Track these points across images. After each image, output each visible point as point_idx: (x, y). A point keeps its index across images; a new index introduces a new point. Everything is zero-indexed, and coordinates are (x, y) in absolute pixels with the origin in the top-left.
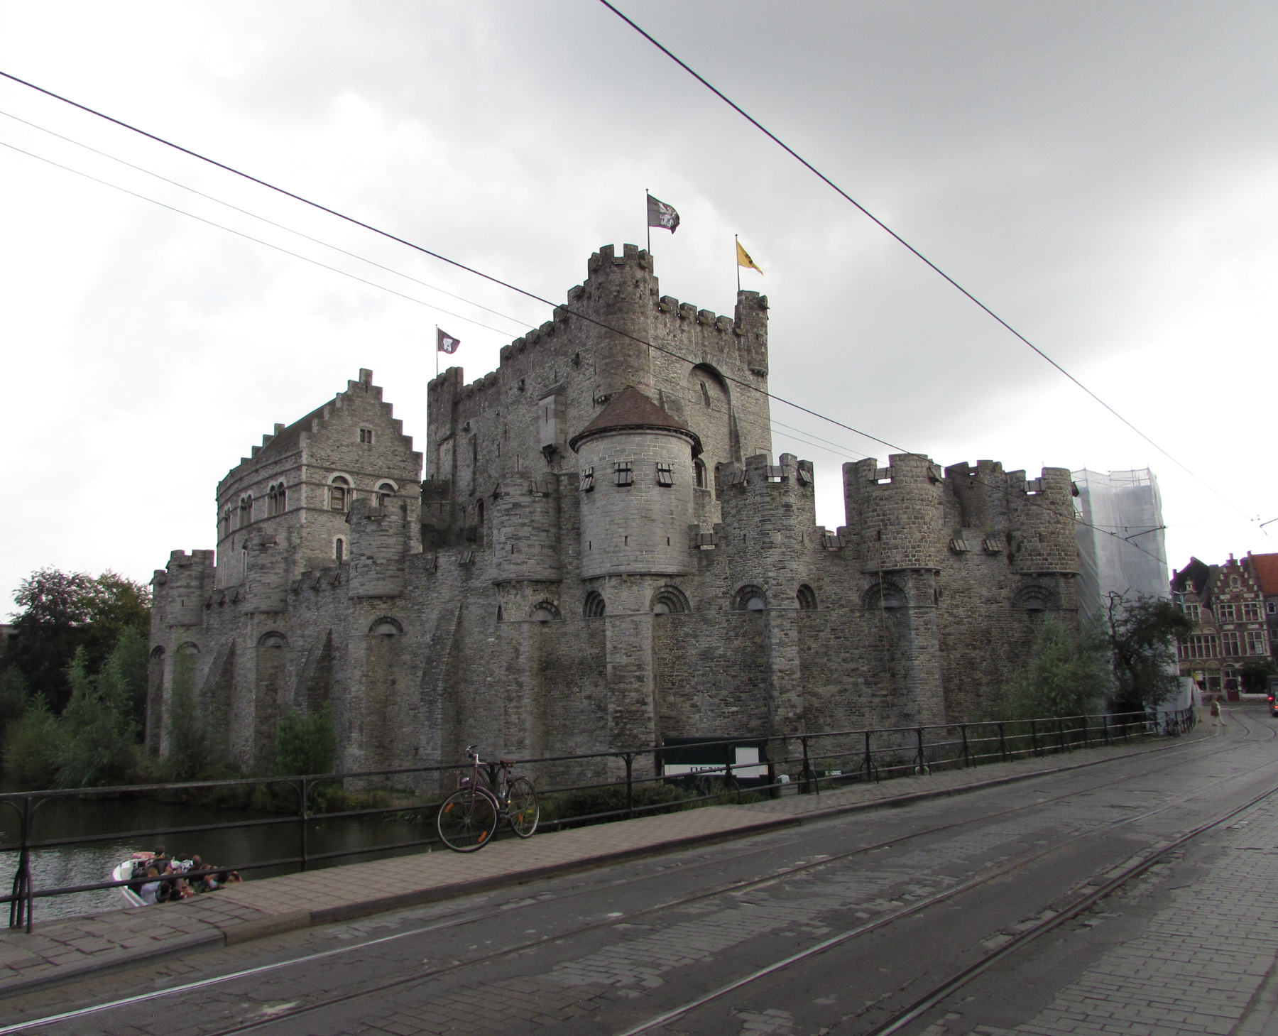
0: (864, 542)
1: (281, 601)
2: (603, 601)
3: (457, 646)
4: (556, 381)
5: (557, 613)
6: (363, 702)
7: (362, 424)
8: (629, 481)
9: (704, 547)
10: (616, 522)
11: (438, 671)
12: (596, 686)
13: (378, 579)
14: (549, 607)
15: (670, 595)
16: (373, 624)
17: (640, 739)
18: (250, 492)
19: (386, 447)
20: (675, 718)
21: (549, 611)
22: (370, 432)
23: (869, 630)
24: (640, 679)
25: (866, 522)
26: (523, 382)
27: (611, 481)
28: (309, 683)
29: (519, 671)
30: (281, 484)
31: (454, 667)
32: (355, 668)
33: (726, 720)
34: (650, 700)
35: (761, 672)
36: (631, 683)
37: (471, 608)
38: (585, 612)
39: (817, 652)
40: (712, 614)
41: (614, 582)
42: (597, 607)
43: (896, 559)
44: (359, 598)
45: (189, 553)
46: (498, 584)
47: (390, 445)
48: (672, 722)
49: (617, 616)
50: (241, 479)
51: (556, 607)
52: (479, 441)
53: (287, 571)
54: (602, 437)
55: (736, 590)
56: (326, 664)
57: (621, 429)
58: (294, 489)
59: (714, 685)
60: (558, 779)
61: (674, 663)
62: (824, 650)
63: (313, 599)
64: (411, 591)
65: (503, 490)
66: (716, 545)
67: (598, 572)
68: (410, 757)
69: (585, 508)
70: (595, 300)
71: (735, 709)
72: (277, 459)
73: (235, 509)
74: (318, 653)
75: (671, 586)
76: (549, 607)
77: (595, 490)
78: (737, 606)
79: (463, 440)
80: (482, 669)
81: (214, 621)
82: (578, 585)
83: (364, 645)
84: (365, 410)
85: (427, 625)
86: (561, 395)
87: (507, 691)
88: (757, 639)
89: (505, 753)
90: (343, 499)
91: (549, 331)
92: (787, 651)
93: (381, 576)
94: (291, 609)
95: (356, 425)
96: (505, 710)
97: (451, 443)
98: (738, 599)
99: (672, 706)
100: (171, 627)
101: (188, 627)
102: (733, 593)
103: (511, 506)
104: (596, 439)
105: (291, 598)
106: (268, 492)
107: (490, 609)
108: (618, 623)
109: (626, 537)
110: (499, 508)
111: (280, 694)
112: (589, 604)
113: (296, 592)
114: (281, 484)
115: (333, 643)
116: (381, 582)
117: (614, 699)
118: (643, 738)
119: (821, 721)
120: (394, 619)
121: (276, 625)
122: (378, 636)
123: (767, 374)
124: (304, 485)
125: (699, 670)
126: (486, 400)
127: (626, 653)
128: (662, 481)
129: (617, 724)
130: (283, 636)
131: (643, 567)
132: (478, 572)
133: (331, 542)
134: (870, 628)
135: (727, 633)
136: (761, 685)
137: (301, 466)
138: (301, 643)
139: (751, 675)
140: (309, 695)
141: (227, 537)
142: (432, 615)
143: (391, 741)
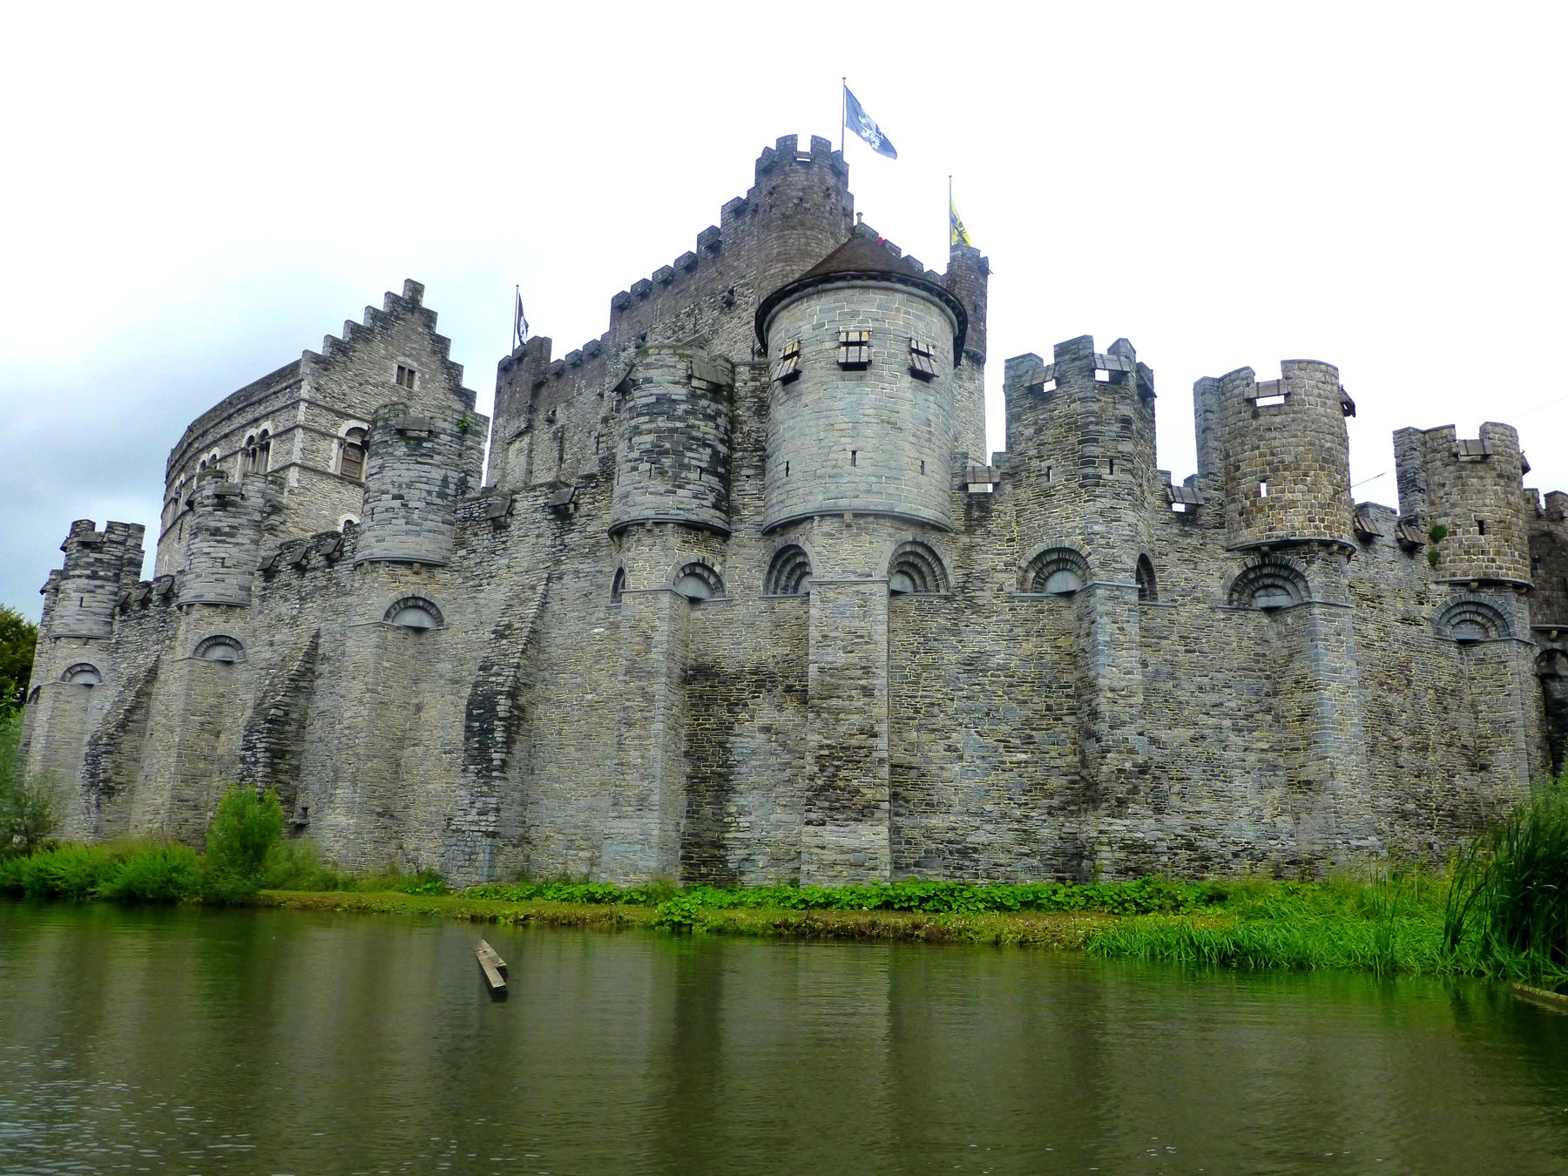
0: (1234, 501)
1: (241, 588)
2: (804, 564)
3: (534, 638)
4: (696, 332)
5: (718, 586)
6: (363, 734)
7: (401, 359)
8: (864, 359)
9: (973, 489)
10: (836, 427)
11: (501, 680)
12: (779, 711)
13: (407, 533)
14: (706, 574)
15: (918, 561)
16: (393, 606)
17: (864, 795)
18: (216, 451)
19: (435, 399)
20: (918, 769)
21: (706, 582)
22: (412, 373)
23: (1239, 647)
24: (867, 692)
25: (1238, 468)
26: (643, 338)
27: (832, 360)
28: (272, 711)
29: (651, 674)
30: (265, 432)
31: (529, 675)
32: (354, 678)
33: (1007, 774)
34: (882, 728)
35: (1068, 696)
36: (851, 698)
37: (566, 579)
38: (766, 586)
39: (1157, 672)
40: (985, 597)
41: (829, 525)
42: (787, 578)
43: (1294, 524)
44: (372, 562)
45: (101, 528)
46: (619, 532)
47: (442, 397)
48: (913, 773)
49: (831, 583)
50: (204, 434)
51: (716, 576)
52: (567, 435)
53: (256, 542)
54: (819, 292)
55: (1031, 559)
56: (302, 684)
57: (854, 278)
58: (284, 437)
59: (988, 714)
60: (704, 870)
61: (918, 676)
62: (1168, 668)
63: (295, 582)
64: (464, 558)
65: (640, 375)
66: (996, 485)
67: (799, 509)
68: (436, 834)
69: (779, 412)
70: (765, 211)
71: (1023, 757)
72: (261, 397)
73: (194, 476)
74: (296, 666)
75: (922, 544)
76: (706, 574)
77: (802, 378)
78: (1028, 585)
79: (543, 434)
80: (579, 680)
81: (132, 634)
82: (758, 540)
83: (374, 639)
84: (407, 338)
85: (486, 611)
86: (702, 348)
87: (625, 709)
88: (1062, 642)
89: (614, 818)
90: (361, 464)
91: (689, 264)
92: (1121, 656)
93: (418, 528)
94: (256, 601)
95: (392, 358)
96: (619, 743)
97: (526, 439)
98: (1032, 574)
99: (912, 747)
100: (57, 638)
101: (87, 639)
102: (1024, 564)
103: (653, 399)
104: (808, 296)
105: (257, 584)
106: (243, 444)
107: (601, 580)
108: (831, 595)
109: (854, 453)
110: (632, 404)
111: (223, 737)
112: (775, 573)
113: (269, 572)
114: (265, 432)
115: (320, 651)
116: (411, 539)
117: (818, 724)
118: (869, 794)
119: (1165, 786)
120: (430, 603)
121: (228, 626)
122: (398, 628)
123: (984, 362)
124: (300, 430)
125: (962, 690)
126: (582, 378)
127: (844, 647)
128: (918, 366)
129: (821, 770)
130: (237, 645)
131: (881, 503)
132: (584, 520)
133: (335, 522)
134: (1241, 639)
135: (1011, 630)
136: (1067, 719)
137: (298, 401)
138: (268, 655)
139: (1051, 702)
140: (270, 731)
141: (174, 524)
142: (495, 596)
143: (406, 807)
